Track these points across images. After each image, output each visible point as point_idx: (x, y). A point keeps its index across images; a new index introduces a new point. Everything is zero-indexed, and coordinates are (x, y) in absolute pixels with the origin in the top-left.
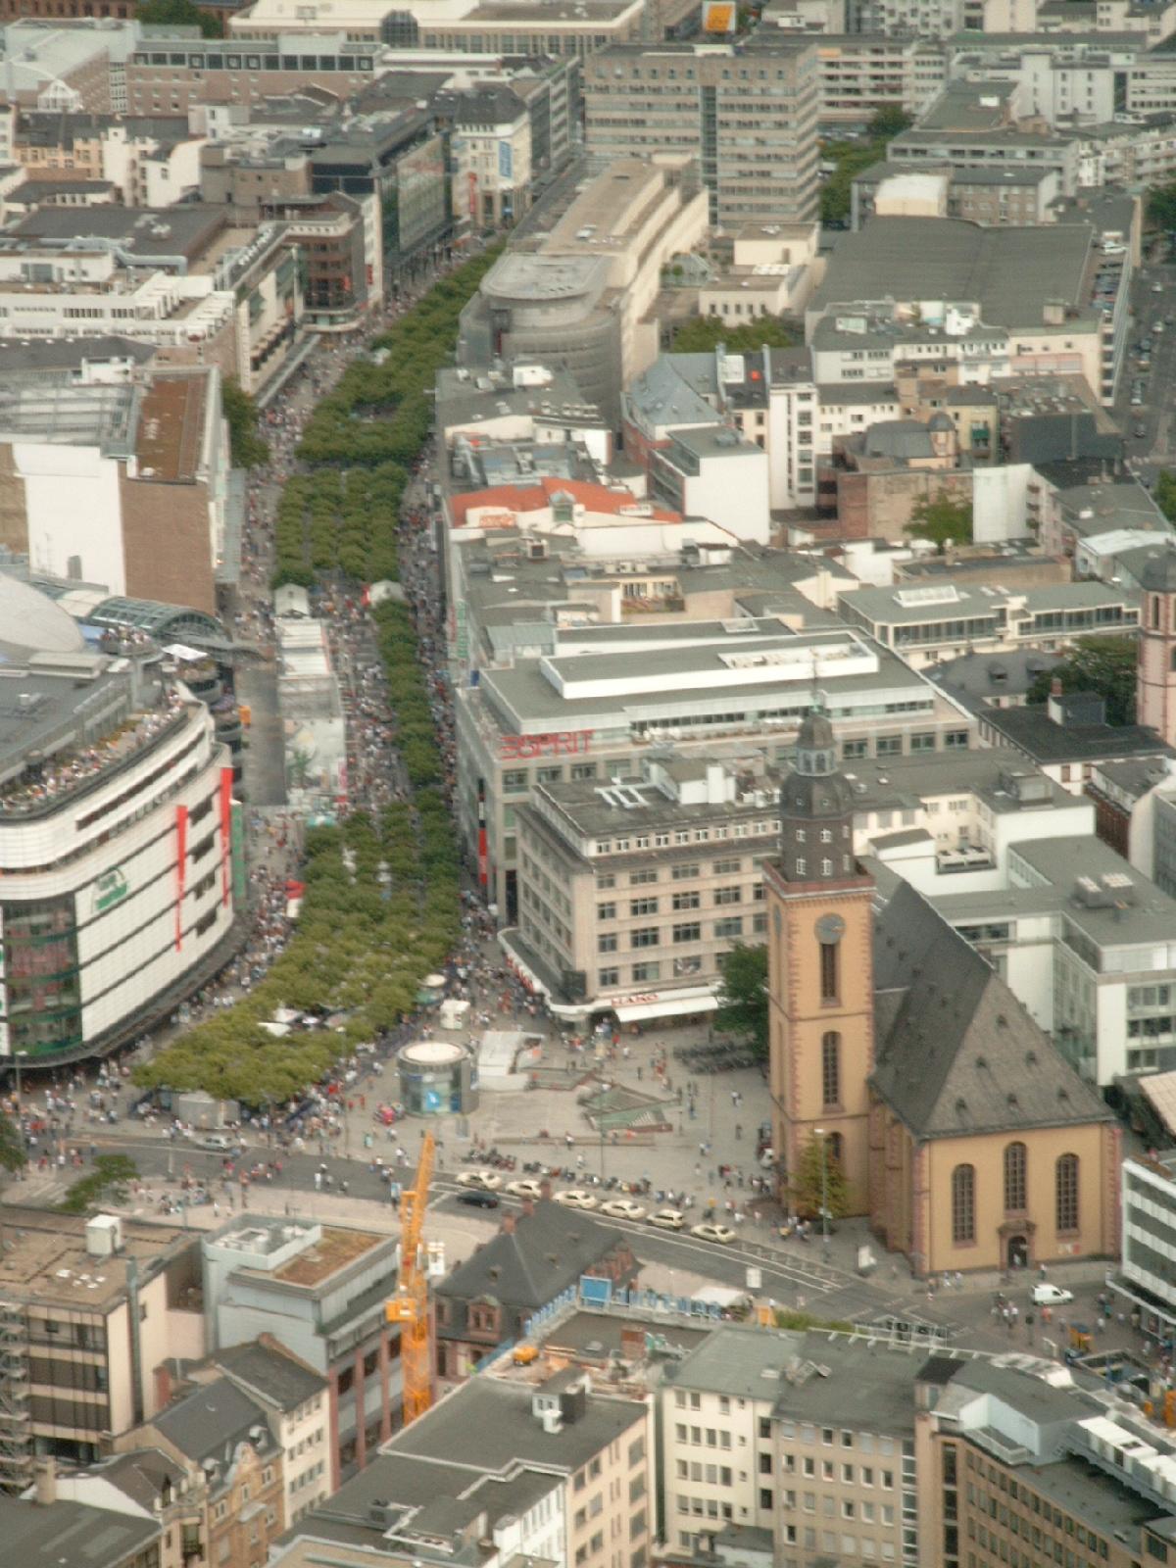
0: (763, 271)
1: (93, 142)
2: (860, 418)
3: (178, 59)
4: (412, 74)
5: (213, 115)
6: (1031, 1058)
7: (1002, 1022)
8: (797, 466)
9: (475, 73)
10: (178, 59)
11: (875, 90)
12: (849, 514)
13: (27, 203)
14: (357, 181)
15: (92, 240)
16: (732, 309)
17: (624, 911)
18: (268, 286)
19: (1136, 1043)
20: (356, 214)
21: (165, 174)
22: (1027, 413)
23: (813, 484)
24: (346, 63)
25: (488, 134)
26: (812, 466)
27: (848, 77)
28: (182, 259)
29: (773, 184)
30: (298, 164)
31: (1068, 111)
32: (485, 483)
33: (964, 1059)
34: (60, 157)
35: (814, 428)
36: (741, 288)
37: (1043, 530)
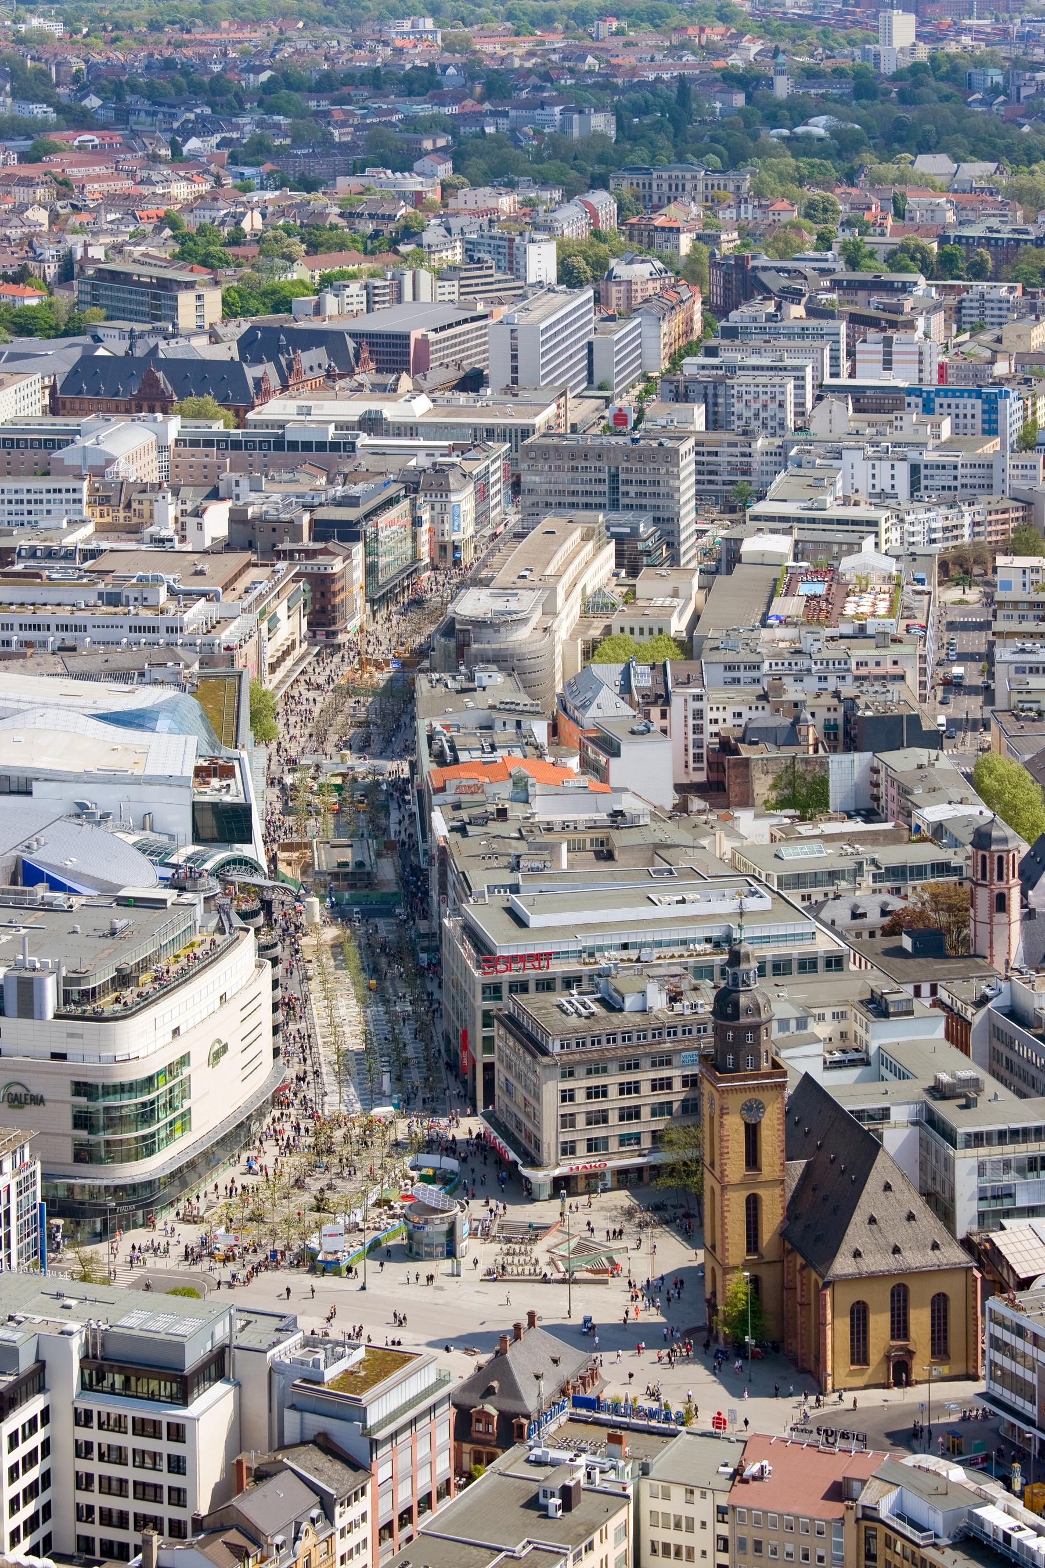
2: (740, 715)
6: (911, 1217)
7: (887, 1187)
8: (691, 751)
12: (734, 791)
14: (348, 532)
17: (580, 1096)
18: (282, 611)
19: (984, 1206)
20: (348, 557)
22: (869, 713)
23: (705, 765)
26: (704, 751)
31: (878, 490)
32: (456, 760)
33: (859, 1217)
35: (705, 722)
37: (882, 802)
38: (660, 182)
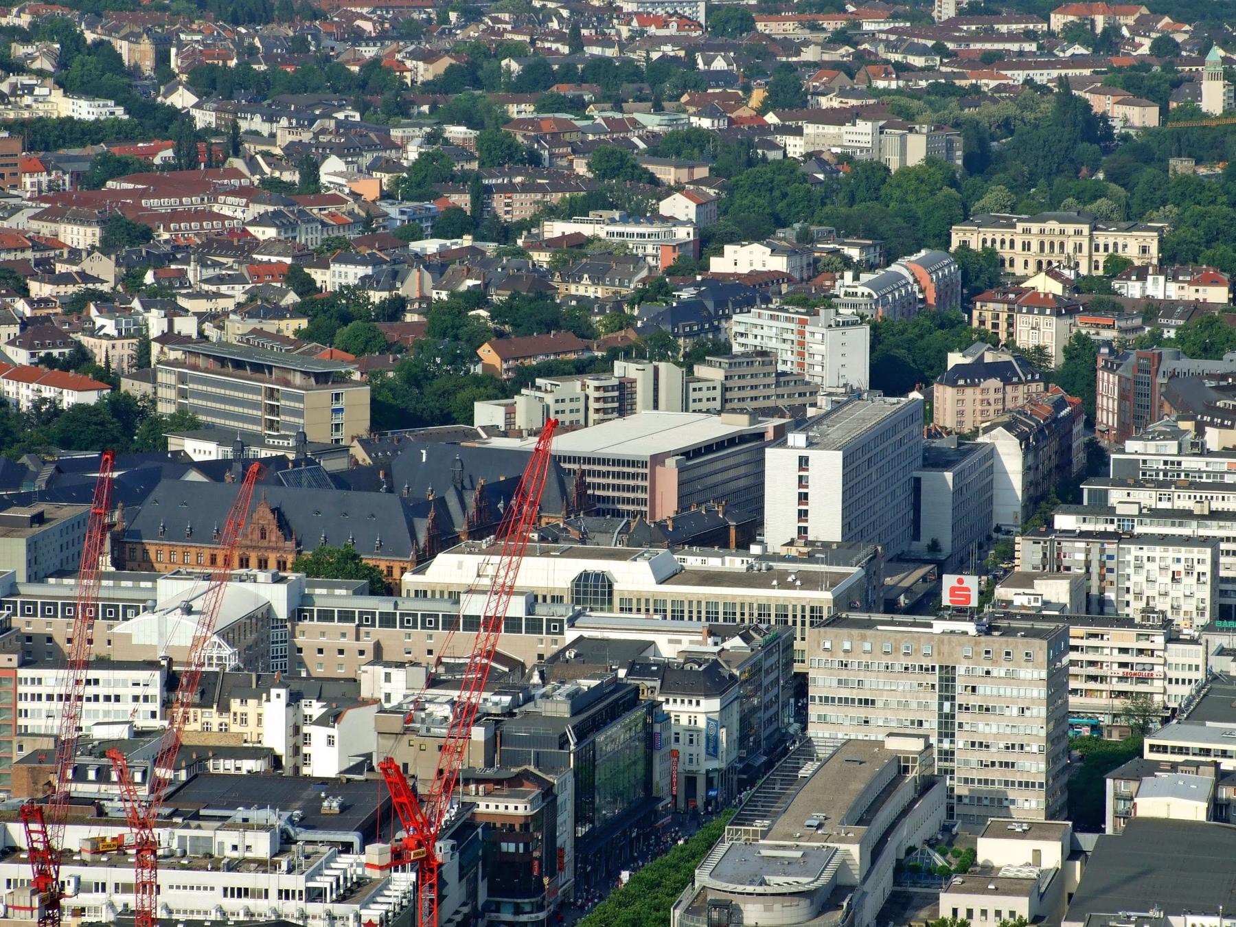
0: (1009, 874)
1: (252, 702)
3: (346, 616)
4: (608, 640)
5: (388, 677)
9: (679, 642)
10: (346, 616)
11: (1122, 679)
13: (177, 769)
15: (256, 815)
16: (976, 913)
21: (330, 741)
24: (534, 626)
25: (694, 708)
27: (1092, 663)
28: (354, 838)
29: (1018, 778)
30: (478, 734)
34: (213, 717)
36: (985, 891)
38: (1027, 238)
